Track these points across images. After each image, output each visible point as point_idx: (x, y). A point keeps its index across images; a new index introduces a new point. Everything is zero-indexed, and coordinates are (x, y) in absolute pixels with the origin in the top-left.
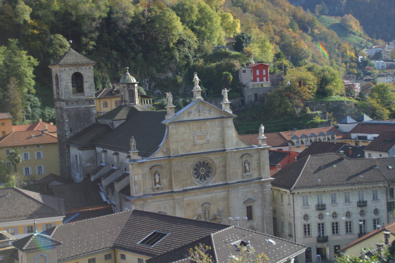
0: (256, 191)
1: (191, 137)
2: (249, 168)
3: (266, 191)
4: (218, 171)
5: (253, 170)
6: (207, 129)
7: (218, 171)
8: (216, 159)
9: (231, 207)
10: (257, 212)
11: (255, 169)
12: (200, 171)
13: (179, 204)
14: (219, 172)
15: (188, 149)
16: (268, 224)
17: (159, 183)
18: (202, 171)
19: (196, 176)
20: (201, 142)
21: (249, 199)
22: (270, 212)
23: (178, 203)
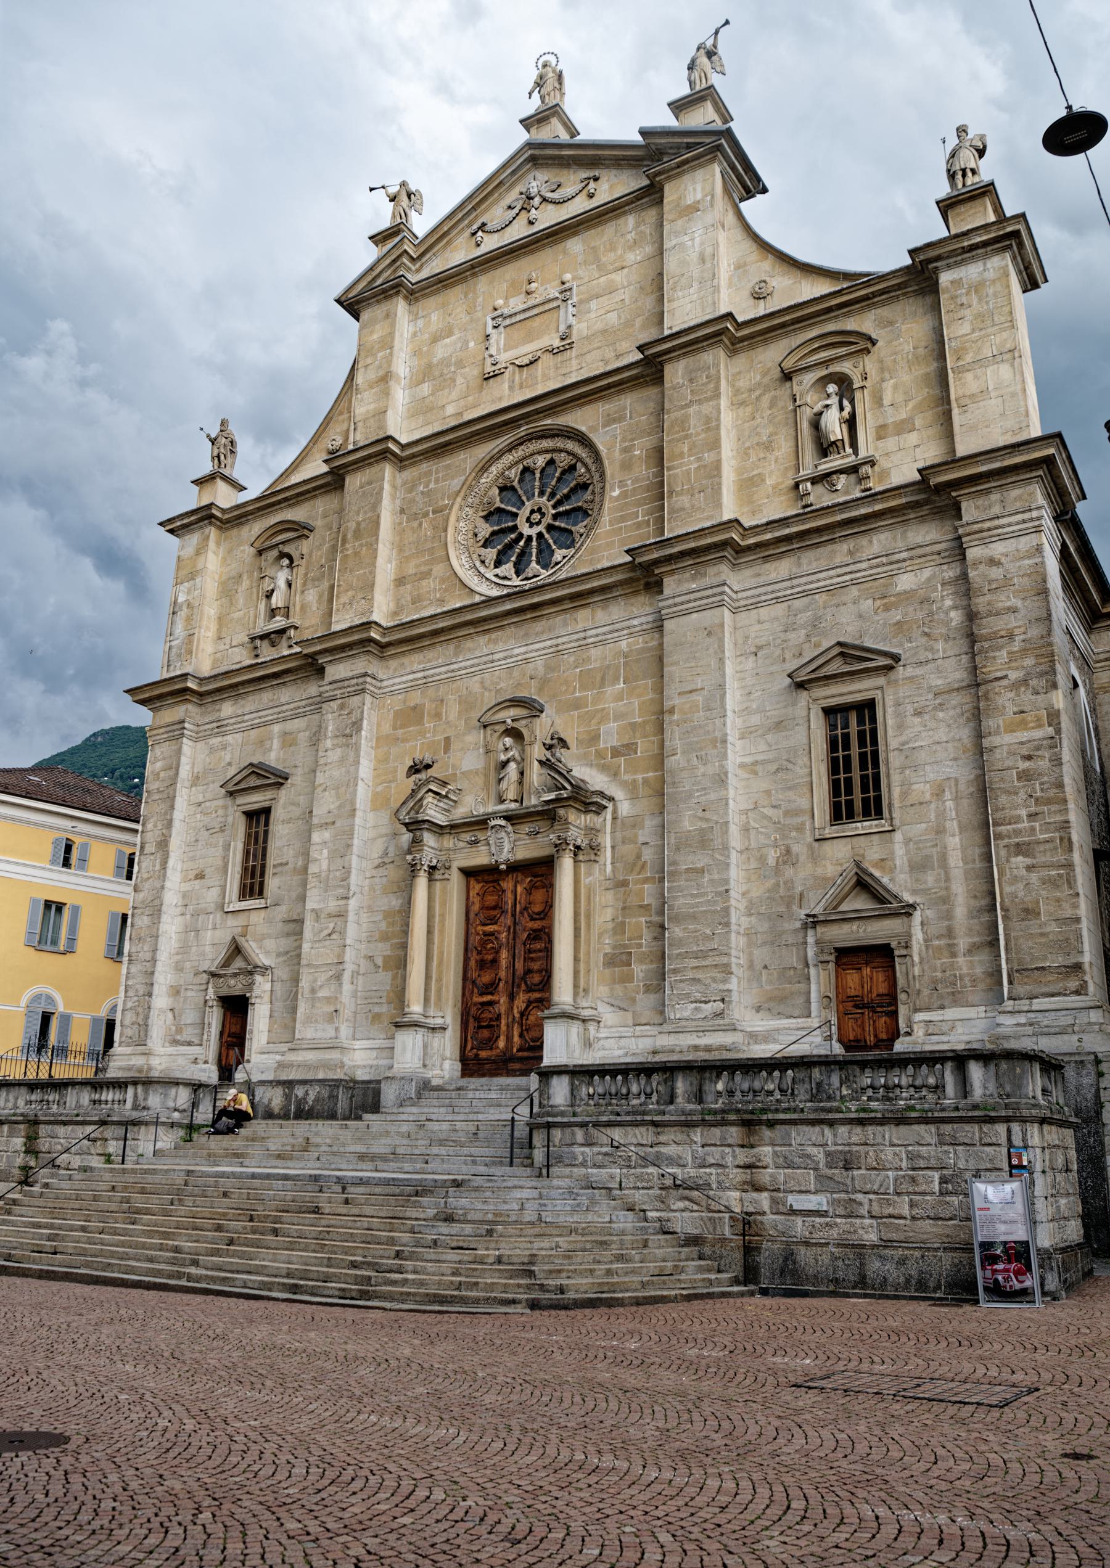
0: (906, 582)
1: (471, 344)
2: (851, 423)
3: (993, 562)
4: (616, 493)
5: (881, 432)
6: (568, 277)
7: (616, 493)
8: (604, 426)
9: (672, 711)
10: (922, 750)
11: (904, 427)
12: (541, 528)
13: (342, 707)
14: (624, 495)
15: (450, 410)
16: (1020, 849)
17: (287, 611)
18: (536, 517)
19: (491, 554)
20: (525, 351)
21: (847, 652)
22: (1051, 731)
23: (334, 705)
